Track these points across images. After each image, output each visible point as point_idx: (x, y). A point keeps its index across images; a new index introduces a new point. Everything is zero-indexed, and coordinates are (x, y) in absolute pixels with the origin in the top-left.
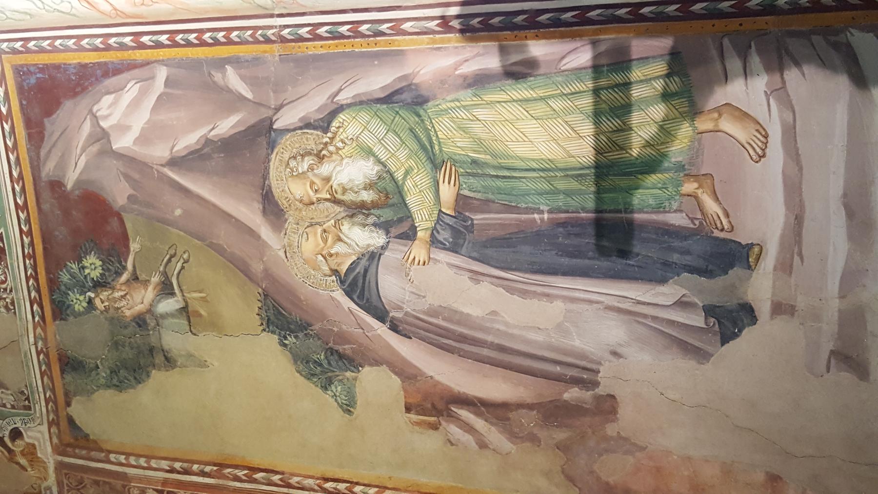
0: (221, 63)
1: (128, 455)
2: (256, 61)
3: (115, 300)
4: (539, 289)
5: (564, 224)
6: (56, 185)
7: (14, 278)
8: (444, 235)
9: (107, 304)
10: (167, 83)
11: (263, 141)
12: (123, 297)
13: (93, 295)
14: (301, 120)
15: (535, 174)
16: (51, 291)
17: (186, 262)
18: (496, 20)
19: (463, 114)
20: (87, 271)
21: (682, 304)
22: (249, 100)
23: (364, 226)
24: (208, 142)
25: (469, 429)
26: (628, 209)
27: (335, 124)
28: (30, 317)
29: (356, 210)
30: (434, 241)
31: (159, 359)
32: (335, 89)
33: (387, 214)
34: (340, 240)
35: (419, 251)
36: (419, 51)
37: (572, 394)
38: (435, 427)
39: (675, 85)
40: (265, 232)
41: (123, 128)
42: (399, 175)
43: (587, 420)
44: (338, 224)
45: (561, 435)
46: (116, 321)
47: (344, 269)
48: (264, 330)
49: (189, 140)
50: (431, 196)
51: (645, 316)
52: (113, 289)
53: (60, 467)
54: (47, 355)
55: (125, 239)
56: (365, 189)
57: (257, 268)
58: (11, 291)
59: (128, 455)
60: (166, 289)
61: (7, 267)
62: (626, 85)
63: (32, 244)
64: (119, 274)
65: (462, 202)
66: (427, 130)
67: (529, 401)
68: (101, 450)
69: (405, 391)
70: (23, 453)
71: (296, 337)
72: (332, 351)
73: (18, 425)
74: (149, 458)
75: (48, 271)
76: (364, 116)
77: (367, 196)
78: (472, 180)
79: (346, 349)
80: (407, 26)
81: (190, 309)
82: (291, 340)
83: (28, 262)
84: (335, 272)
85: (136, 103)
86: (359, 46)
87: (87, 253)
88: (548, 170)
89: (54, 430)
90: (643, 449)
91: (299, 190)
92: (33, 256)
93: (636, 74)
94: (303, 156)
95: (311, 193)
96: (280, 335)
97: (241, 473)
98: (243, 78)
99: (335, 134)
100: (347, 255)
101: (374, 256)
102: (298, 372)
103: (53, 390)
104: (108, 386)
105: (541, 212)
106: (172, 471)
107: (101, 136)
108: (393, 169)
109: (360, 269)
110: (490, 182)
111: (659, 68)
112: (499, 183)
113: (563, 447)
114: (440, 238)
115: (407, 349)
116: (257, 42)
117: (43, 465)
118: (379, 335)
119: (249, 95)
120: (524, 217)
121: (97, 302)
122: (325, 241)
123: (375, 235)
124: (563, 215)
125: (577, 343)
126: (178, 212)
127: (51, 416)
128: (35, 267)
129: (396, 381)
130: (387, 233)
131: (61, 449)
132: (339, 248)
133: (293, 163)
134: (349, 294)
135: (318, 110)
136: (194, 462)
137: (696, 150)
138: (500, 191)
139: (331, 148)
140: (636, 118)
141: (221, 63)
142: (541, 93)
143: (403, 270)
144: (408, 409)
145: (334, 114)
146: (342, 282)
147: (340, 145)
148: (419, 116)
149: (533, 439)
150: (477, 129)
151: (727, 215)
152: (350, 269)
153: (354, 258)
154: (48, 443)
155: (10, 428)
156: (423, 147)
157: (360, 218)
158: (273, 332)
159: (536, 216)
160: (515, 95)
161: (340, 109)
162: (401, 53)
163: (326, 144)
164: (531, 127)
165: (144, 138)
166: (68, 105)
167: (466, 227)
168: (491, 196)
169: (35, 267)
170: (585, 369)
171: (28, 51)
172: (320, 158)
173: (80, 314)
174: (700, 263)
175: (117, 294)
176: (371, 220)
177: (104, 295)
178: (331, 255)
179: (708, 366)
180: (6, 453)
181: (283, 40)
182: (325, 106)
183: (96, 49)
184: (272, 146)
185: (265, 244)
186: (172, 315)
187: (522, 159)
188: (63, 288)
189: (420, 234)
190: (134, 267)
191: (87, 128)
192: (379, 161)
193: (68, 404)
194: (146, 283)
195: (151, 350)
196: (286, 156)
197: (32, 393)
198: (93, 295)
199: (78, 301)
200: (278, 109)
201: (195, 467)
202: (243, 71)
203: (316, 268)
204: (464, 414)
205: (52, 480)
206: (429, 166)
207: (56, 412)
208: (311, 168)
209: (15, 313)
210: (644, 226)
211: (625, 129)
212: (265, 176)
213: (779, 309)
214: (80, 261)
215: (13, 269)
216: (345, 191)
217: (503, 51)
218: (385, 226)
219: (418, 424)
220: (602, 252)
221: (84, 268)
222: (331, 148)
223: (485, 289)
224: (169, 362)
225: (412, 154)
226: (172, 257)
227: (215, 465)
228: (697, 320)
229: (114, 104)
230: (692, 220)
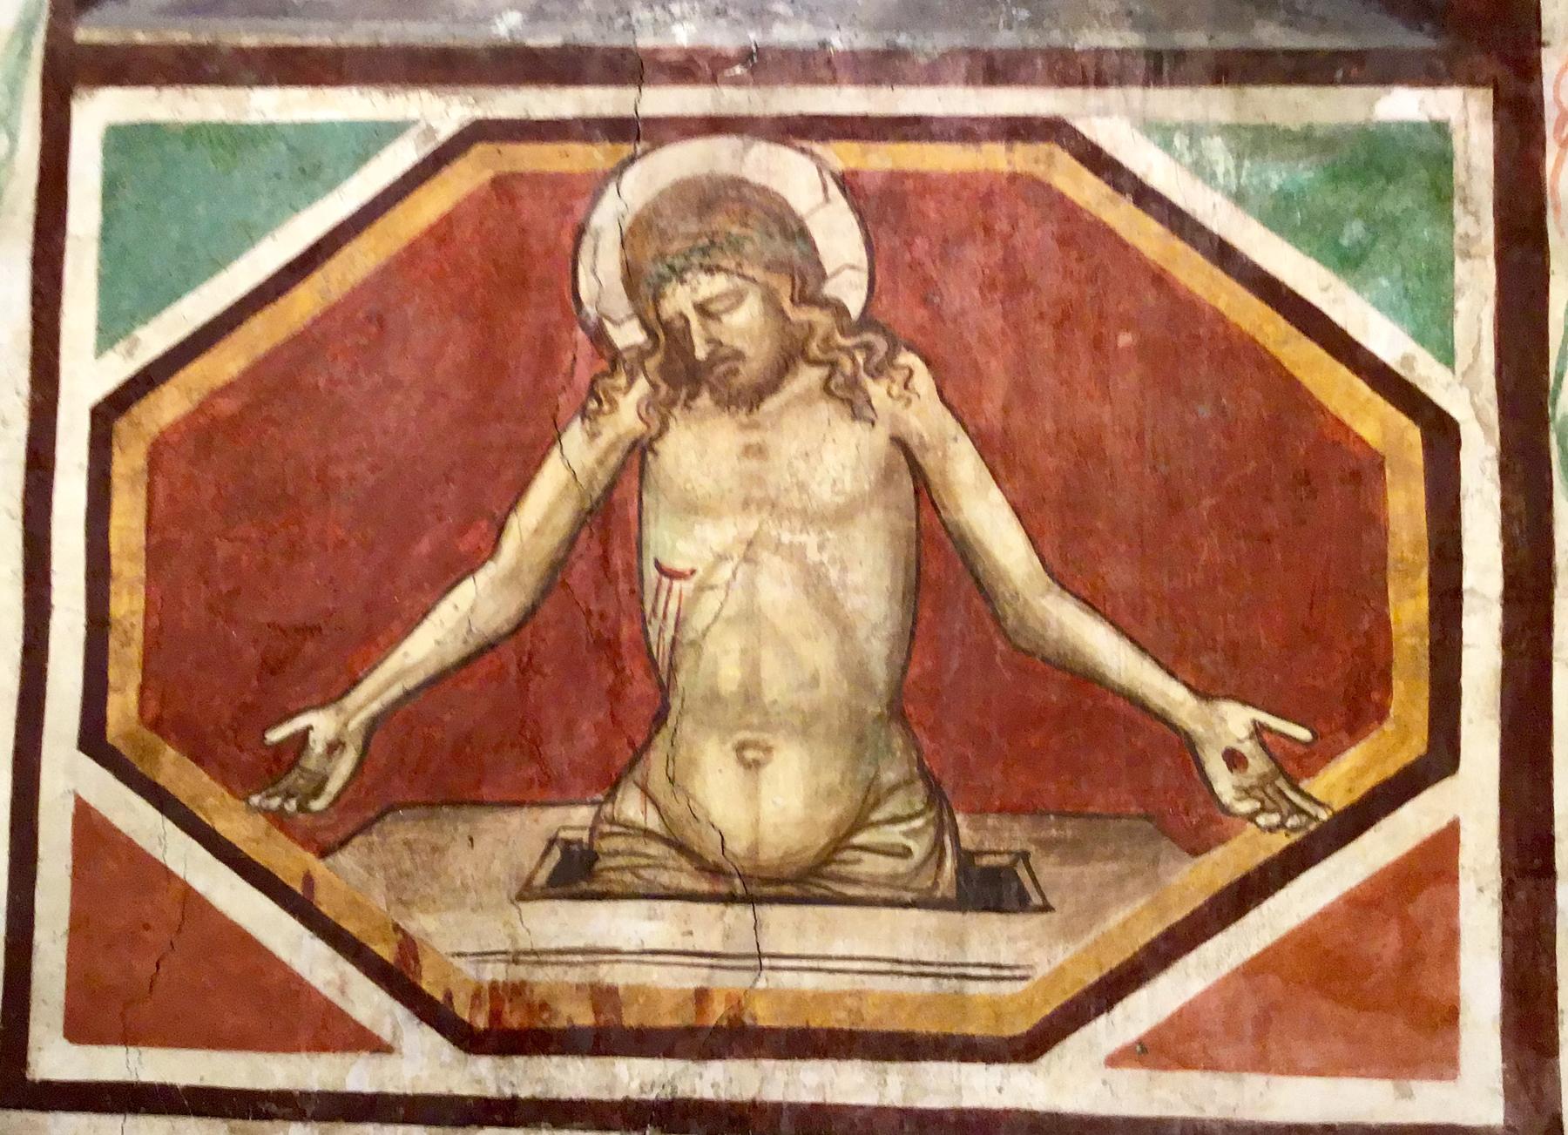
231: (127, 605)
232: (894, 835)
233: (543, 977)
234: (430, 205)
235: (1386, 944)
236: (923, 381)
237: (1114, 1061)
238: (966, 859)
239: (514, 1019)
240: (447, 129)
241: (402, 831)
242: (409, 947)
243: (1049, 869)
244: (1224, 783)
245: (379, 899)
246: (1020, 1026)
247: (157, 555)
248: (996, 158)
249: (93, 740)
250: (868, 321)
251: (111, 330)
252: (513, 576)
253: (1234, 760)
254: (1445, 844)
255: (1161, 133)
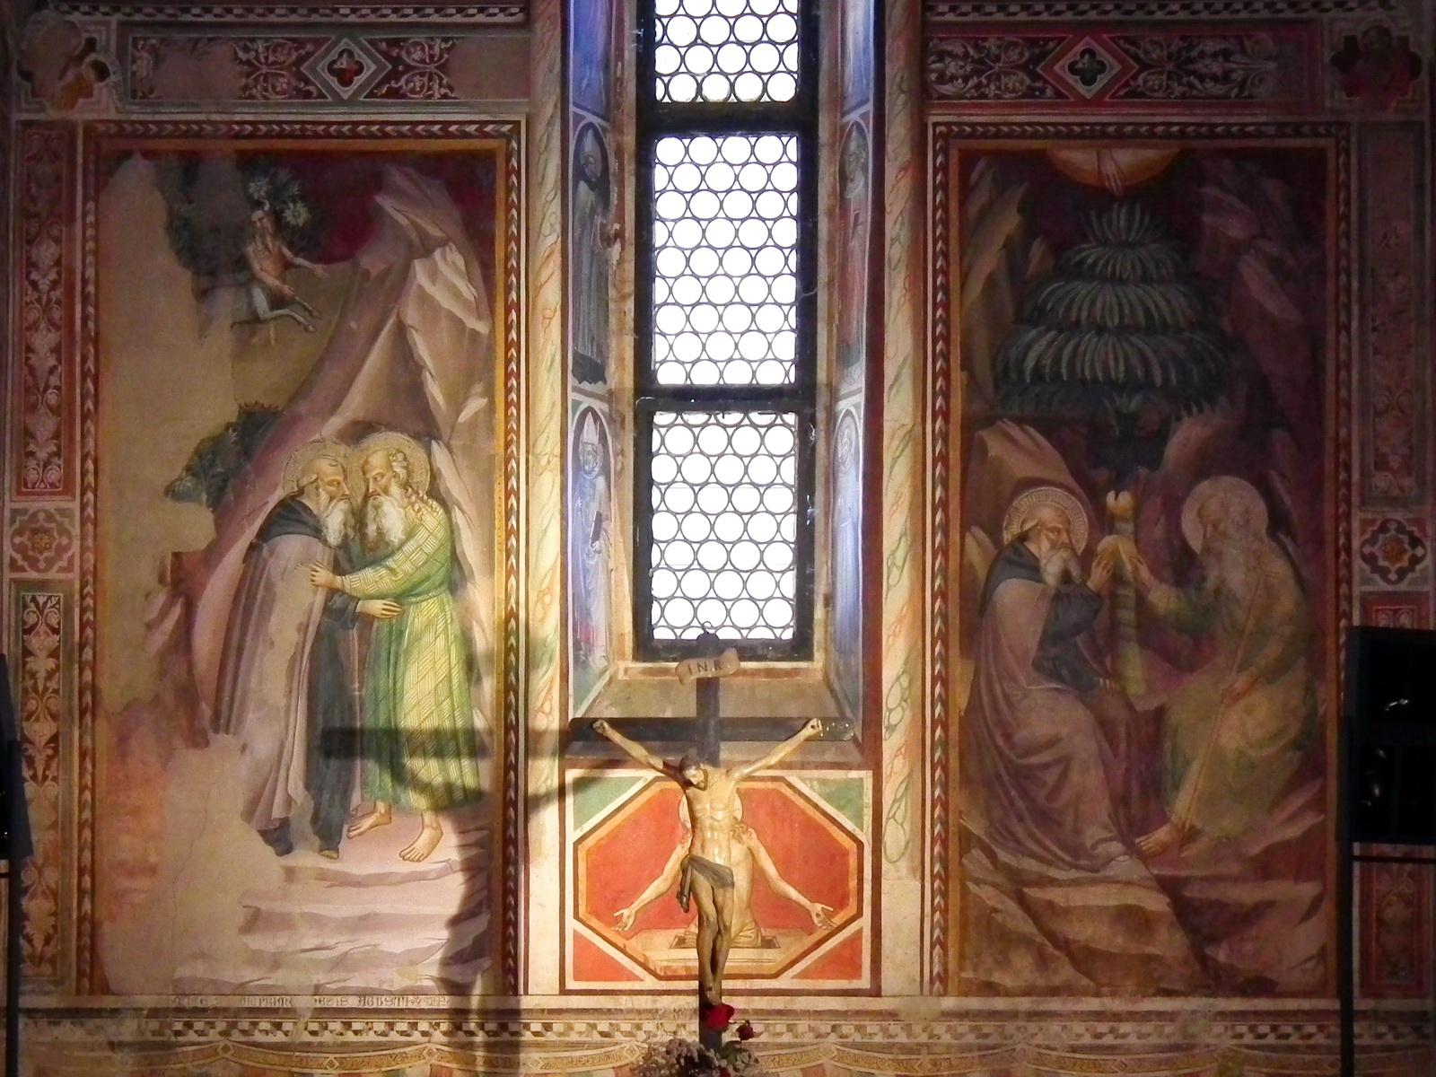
0: (489, 393)
1: (96, 225)
2: (491, 430)
3: (263, 236)
4: (295, 685)
5: (351, 707)
6: (377, 183)
7: (277, 105)
8: (338, 601)
9: (258, 224)
10: (474, 333)
11: (420, 427)
12: (267, 247)
13: (267, 207)
14: (439, 470)
15: (391, 685)
16: (265, 152)
17: (306, 329)
18: (513, 657)
19: (441, 625)
20: (291, 205)
21: (289, 801)
22: (458, 415)
23: (345, 525)
24: (420, 368)
25: (164, 613)
26: (363, 755)
27: (435, 504)
28: (238, 118)
29: (358, 518)
30: (333, 592)
31: (205, 282)
32: (464, 507)
33: (356, 548)
34: (332, 499)
35: (324, 576)
36: (493, 590)
37: (206, 710)
38: (161, 579)
39: (458, 795)
40: (336, 423)
41: (434, 275)
42: (390, 563)
43: (184, 722)
44: (345, 497)
45: (169, 699)
46: (241, 232)
47: (306, 501)
48: (240, 407)
49: (423, 350)
50: (372, 590)
51: (278, 771)
52: (274, 236)
53: (70, 127)
54: (198, 135)
55: (327, 259)
56: (378, 528)
57: (303, 407)
58: (265, 98)
59: (96, 225)
60: (277, 301)
61: (290, 98)
62: (458, 755)
63: (316, 136)
64: (291, 246)
65: (367, 620)
66: (427, 592)
67: (195, 672)
68: (97, 192)
69: (194, 553)
70: (79, 77)
71: (236, 442)
72: (225, 481)
73: (113, 78)
74: (96, 253)
75: (290, 152)
76: (441, 533)
77: (371, 529)
78: (386, 630)
79: (230, 497)
80: (513, 580)
81: (259, 326)
82: (233, 436)
83: (298, 127)
84: (301, 491)
85: (457, 295)
86: (499, 534)
87: (311, 210)
88: (395, 695)
89: (114, 129)
90: (164, 768)
91: (377, 461)
92: (303, 136)
93: (466, 762)
94: (406, 468)
95: (374, 473)
96: (237, 424)
97: (90, 364)
98: (477, 414)
99: (426, 503)
100: (318, 504)
101: (317, 532)
102: (202, 441)
103: (157, 136)
104: (170, 212)
105: (360, 689)
106: (85, 282)
107: (425, 248)
108: (396, 557)
109: (306, 517)
110: (385, 645)
111: (470, 782)
112: (384, 655)
113: (157, 699)
114: (336, 598)
115: (233, 558)
116: (507, 433)
117: (71, 105)
118: (244, 532)
119: (464, 416)
120: (356, 674)
121: (259, 214)
122: (331, 483)
123: (337, 534)
124: (358, 708)
125: (251, 716)
126: (353, 325)
127: (128, 128)
128: (291, 136)
129: (203, 545)
130: (339, 547)
131: (89, 128)
132: (324, 497)
133: (400, 457)
134: (282, 503)
135: (448, 490)
136: (97, 309)
137: (409, 811)
138: (378, 655)
139: (414, 498)
140: (433, 764)
141: (489, 393)
142: (456, 693)
143: (307, 560)
144: (177, 555)
145: (443, 503)
146: (293, 498)
147: (417, 507)
148: (440, 585)
149: (162, 674)
150: (428, 637)
151: (359, 834)
152: (306, 508)
153: (315, 512)
154: (94, 116)
155: (108, 64)
156: (414, 587)
157: (352, 521)
158: (239, 417)
159: (357, 685)
160: (455, 672)
161: (448, 511)
162: (491, 572)
163: (417, 493)
164: (429, 684)
165: (424, 298)
166: (456, 214)
167: (345, 623)
168: (372, 647)
169: (291, 136)
170: (229, 721)
171: (508, 174)
172: (406, 485)
173: (246, 188)
174: (322, 814)
175: (269, 239)
176: (351, 533)
177: (267, 223)
178: (317, 488)
179: (238, 823)
180: (77, 52)
181: (507, 462)
182: (451, 496)
183: (507, 259)
184: (416, 436)
185: (325, 419)
186: (250, 303)
187: (403, 674)
188: (272, 170)
189: (338, 578)
190: (299, 266)
191: (434, 232)
192: (402, 544)
193: (148, 154)
194: (282, 278)
195: (212, 274)
196: (407, 451)
197: (152, 105)
198: (267, 207)
199: (258, 188)
200: (448, 447)
201: (91, 310)
202: (482, 415)
203: (304, 472)
204: (177, 611)
205: (52, 114)
206: (398, 591)
207: (134, 135)
208: (396, 476)
209: (240, 98)
210: (350, 771)
211: (425, 754)
212: (392, 427)
213: (290, 874)
214: (303, 198)
215: (285, 104)
216: (377, 508)
217: (490, 657)
218: (344, 545)
219: (162, 563)
220: (328, 735)
221: (295, 202)
222: (414, 498)
223: (293, 637)
224: (203, 294)
225: (408, 575)
226: (310, 312)
227: (97, 334)
228: (277, 813)
229: (456, 268)
230: (356, 809)
231: (582, 886)
232: (748, 933)
233: (674, 965)
234: (647, 795)
235: (847, 953)
236: (754, 835)
237: (793, 978)
238: (763, 938)
239: (669, 973)
240: (650, 778)
241: (644, 935)
242: (646, 958)
243: (780, 940)
244: (816, 920)
245: (640, 948)
246: (773, 972)
247: (588, 876)
248: (770, 785)
249: (576, 916)
250: (742, 821)
251: (578, 824)
252: (666, 879)
253: (818, 915)
254: (860, 931)
255: (803, 780)
